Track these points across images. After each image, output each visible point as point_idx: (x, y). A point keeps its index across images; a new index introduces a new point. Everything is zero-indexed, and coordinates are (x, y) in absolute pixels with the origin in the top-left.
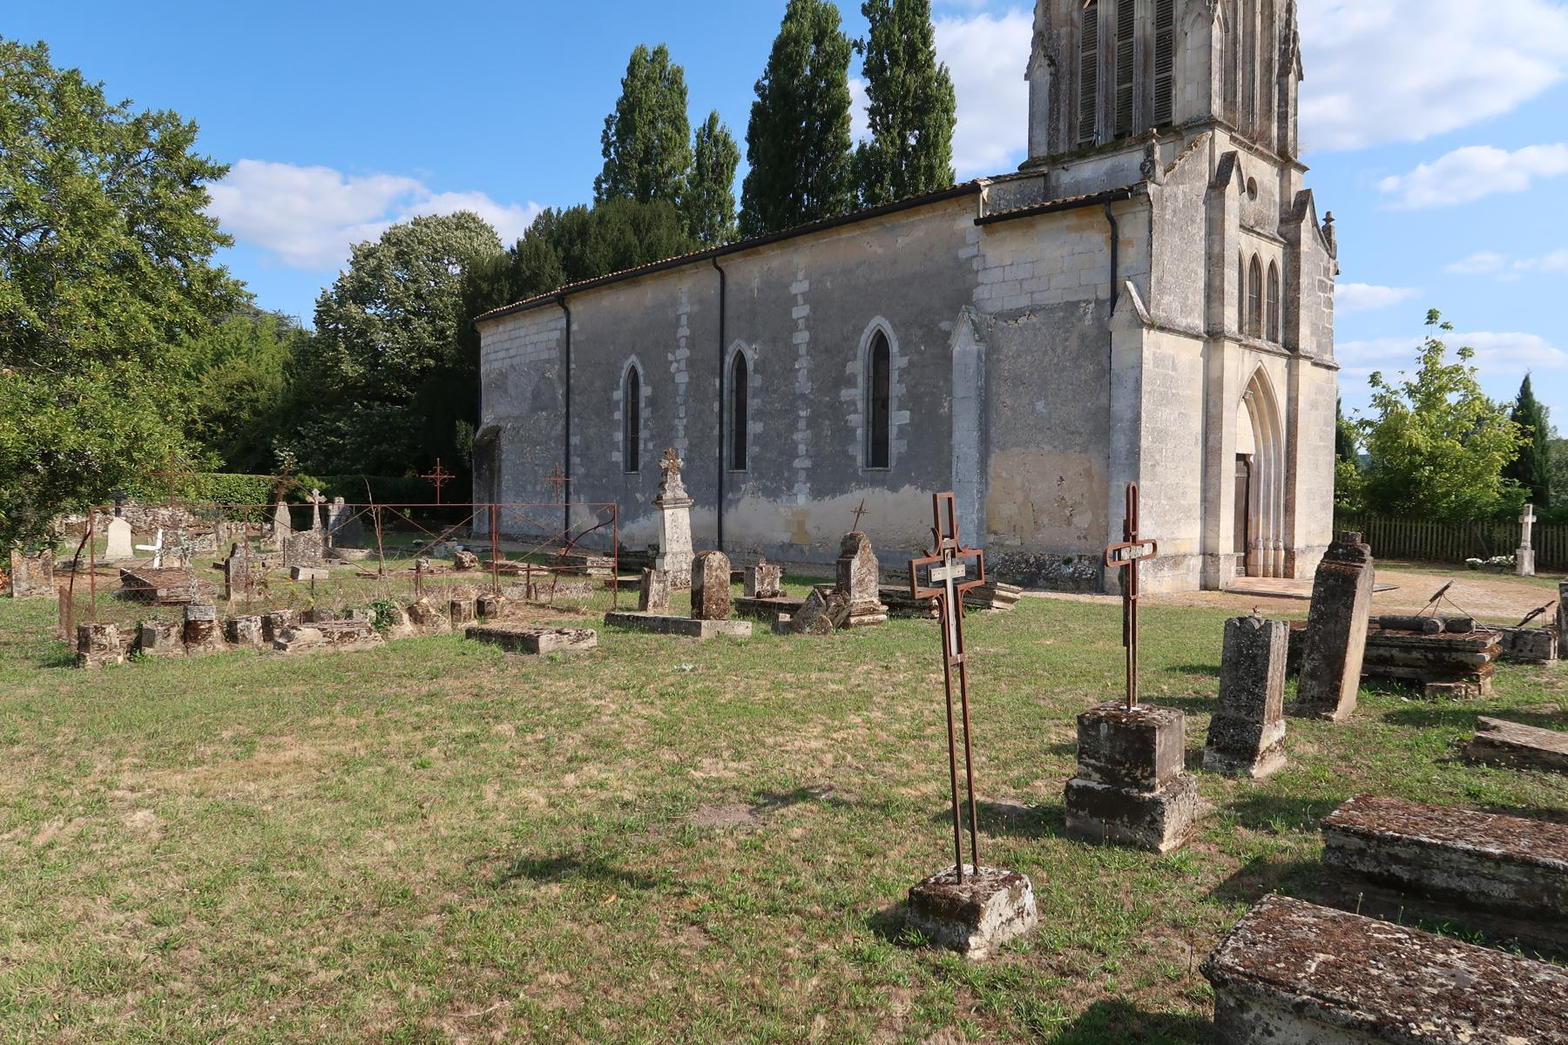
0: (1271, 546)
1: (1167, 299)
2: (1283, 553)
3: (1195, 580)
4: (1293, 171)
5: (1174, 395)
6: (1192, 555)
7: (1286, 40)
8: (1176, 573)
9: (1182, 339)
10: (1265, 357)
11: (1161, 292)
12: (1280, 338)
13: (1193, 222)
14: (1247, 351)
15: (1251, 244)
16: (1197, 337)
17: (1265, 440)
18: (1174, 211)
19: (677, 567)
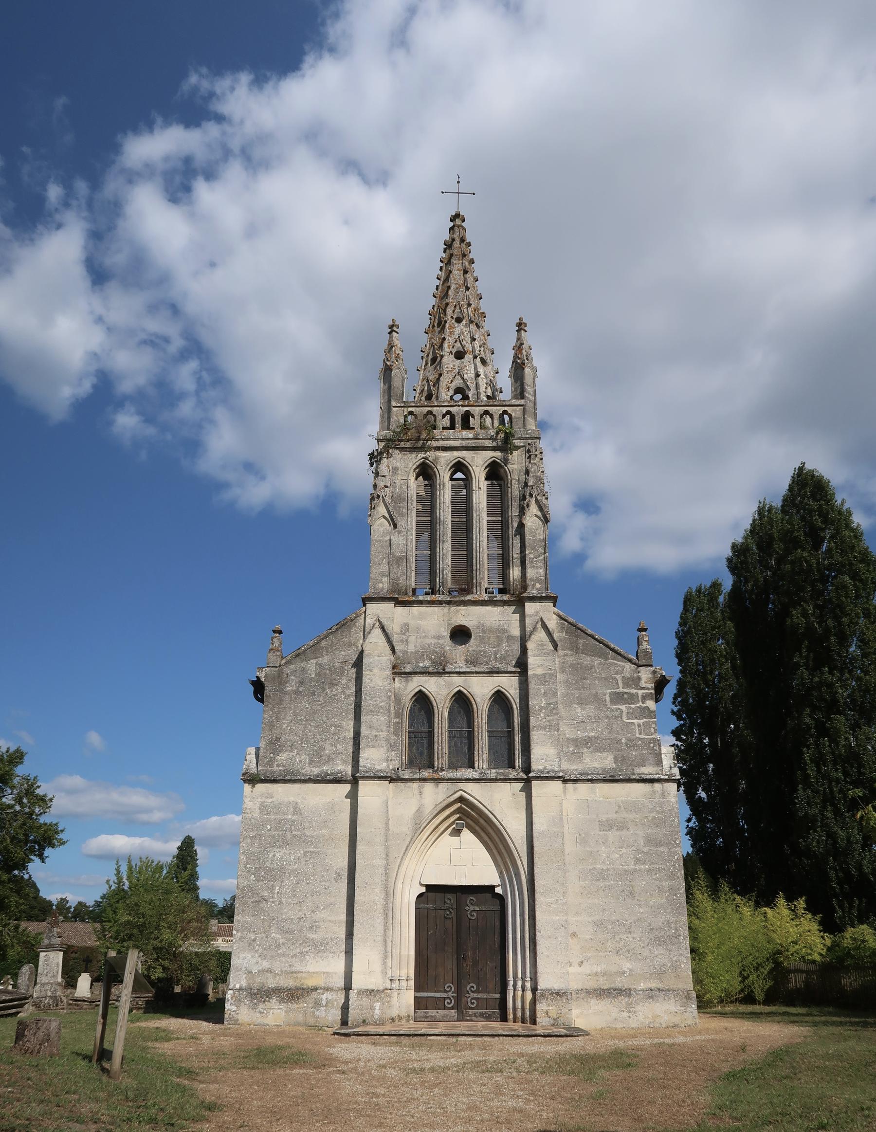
0: (520, 983)
1: (283, 757)
2: (529, 995)
3: (335, 1015)
4: (528, 605)
5: (295, 836)
6: (327, 989)
7: (524, 498)
8: (295, 1006)
9: (311, 786)
10: (471, 788)
11: (277, 752)
12: (518, 762)
13: (332, 685)
14: (429, 787)
15: (449, 685)
16: (337, 781)
17: (508, 871)
18: (302, 683)
19: (43, 994)
